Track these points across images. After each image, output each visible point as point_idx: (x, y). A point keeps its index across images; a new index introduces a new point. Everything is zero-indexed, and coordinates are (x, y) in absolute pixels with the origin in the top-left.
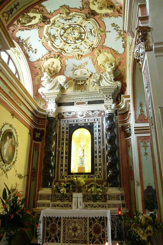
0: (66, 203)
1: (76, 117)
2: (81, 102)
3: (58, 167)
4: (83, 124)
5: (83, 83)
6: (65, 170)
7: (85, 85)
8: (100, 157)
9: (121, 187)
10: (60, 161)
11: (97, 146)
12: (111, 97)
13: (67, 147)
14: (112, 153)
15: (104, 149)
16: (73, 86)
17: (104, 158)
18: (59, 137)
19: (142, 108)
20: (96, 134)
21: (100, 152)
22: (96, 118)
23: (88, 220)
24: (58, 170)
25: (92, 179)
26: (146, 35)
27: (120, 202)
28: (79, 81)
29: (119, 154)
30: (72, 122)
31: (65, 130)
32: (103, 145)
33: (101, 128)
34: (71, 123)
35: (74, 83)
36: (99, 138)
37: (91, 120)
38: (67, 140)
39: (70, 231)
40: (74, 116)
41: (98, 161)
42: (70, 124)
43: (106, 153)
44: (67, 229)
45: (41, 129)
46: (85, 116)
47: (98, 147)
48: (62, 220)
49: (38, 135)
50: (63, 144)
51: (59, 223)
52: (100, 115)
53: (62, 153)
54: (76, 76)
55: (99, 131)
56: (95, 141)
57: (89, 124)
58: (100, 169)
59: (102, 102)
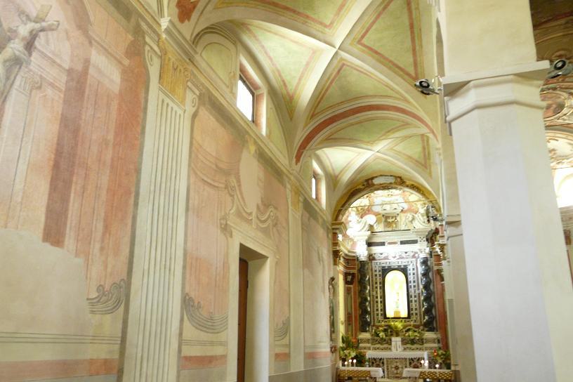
0: (386, 346)
1: (388, 259)
3: (374, 311)
4: (396, 267)
5: (393, 220)
6: (382, 315)
8: (415, 301)
9: (437, 331)
10: (375, 306)
11: (412, 290)
12: (425, 239)
13: (382, 290)
14: (427, 299)
15: (419, 294)
17: (420, 303)
18: (372, 281)
20: (411, 278)
21: (415, 296)
22: (410, 260)
23: (408, 360)
24: (374, 314)
25: (408, 323)
27: (436, 345)
29: (434, 299)
30: (385, 263)
31: (377, 273)
32: (418, 290)
33: (415, 271)
34: (384, 265)
35: (383, 219)
36: (414, 282)
37: (402, 263)
38: (380, 283)
39: (393, 369)
40: (386, 258)
41: (414, 305)
42: (383, 267)
43: (422, 298)
44: (389, 368)
45: (352, 271)
46: (398, 257)
47: (413, 291)
48: (385, 360)
49: (349, 278)
50: (376, 287)
51: (383, 363)
52: (414, 257)
53: (377, 297)
54: (385, 211)
55: (414, 274)
56: (410, 284)
57: (402, 267)
58: (416, 314)
59: (415, 242)
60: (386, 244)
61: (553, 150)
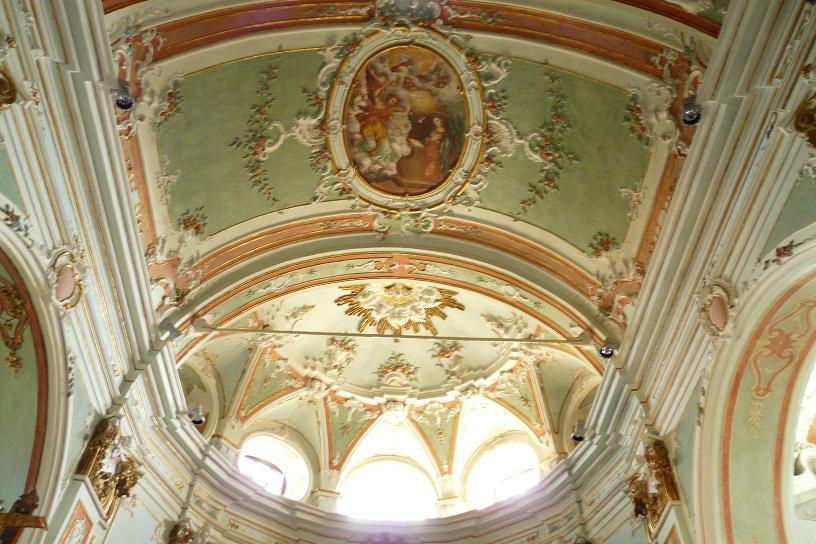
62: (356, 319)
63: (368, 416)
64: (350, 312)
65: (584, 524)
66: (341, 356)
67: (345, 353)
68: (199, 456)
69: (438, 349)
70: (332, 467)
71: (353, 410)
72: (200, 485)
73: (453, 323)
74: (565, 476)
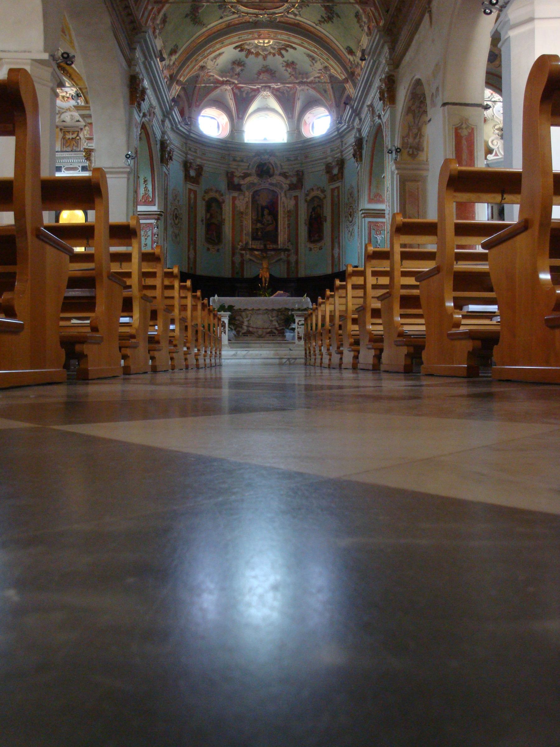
2: (71, 166)
5: (74, 136)
7: (78, 139)
16: (60, 140)
19: (147, 186)
26: (90, 155)
28: (69, 132)
35: (61, 135)
54: (64, 123)
60: (63, 169)
61: (293, 63)
62: (244, 53)
63: (253, 94)
64: (241, 50)
65: (342, 152)
66: (238, 69)
67: (240, 68)
68: (187, 133)
69: (285, 64)
70: (238, 118)
71: (246, 92)
72: (189, 142)
73: (290, 55)
74: (336, 133)
